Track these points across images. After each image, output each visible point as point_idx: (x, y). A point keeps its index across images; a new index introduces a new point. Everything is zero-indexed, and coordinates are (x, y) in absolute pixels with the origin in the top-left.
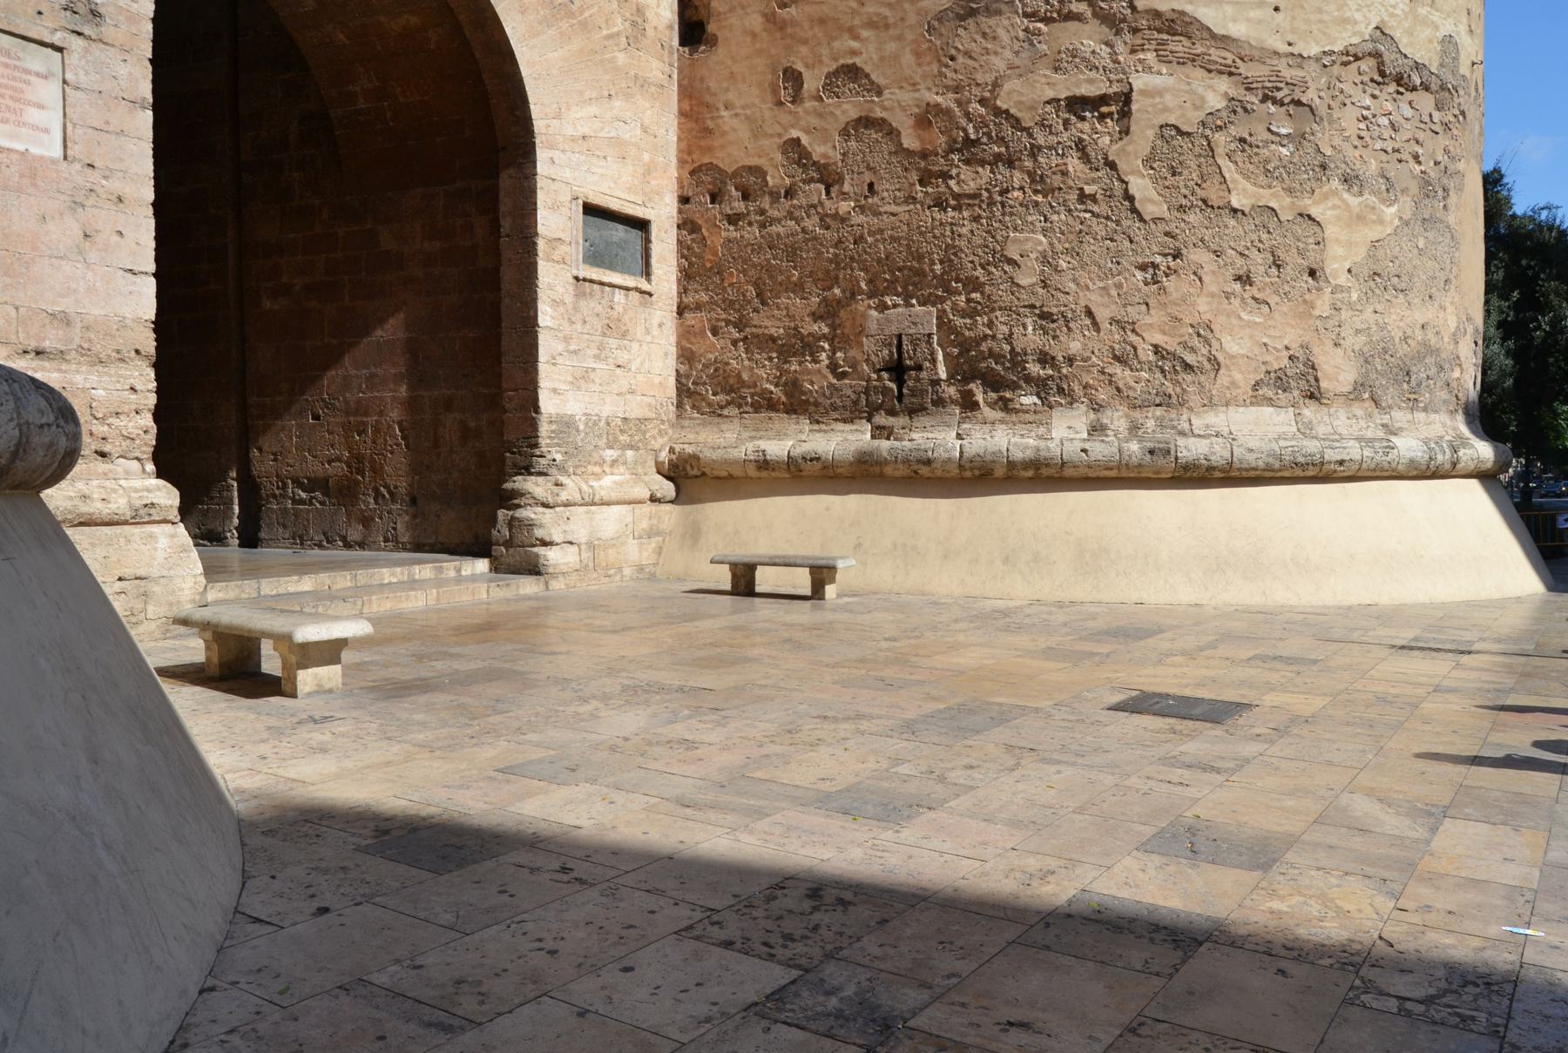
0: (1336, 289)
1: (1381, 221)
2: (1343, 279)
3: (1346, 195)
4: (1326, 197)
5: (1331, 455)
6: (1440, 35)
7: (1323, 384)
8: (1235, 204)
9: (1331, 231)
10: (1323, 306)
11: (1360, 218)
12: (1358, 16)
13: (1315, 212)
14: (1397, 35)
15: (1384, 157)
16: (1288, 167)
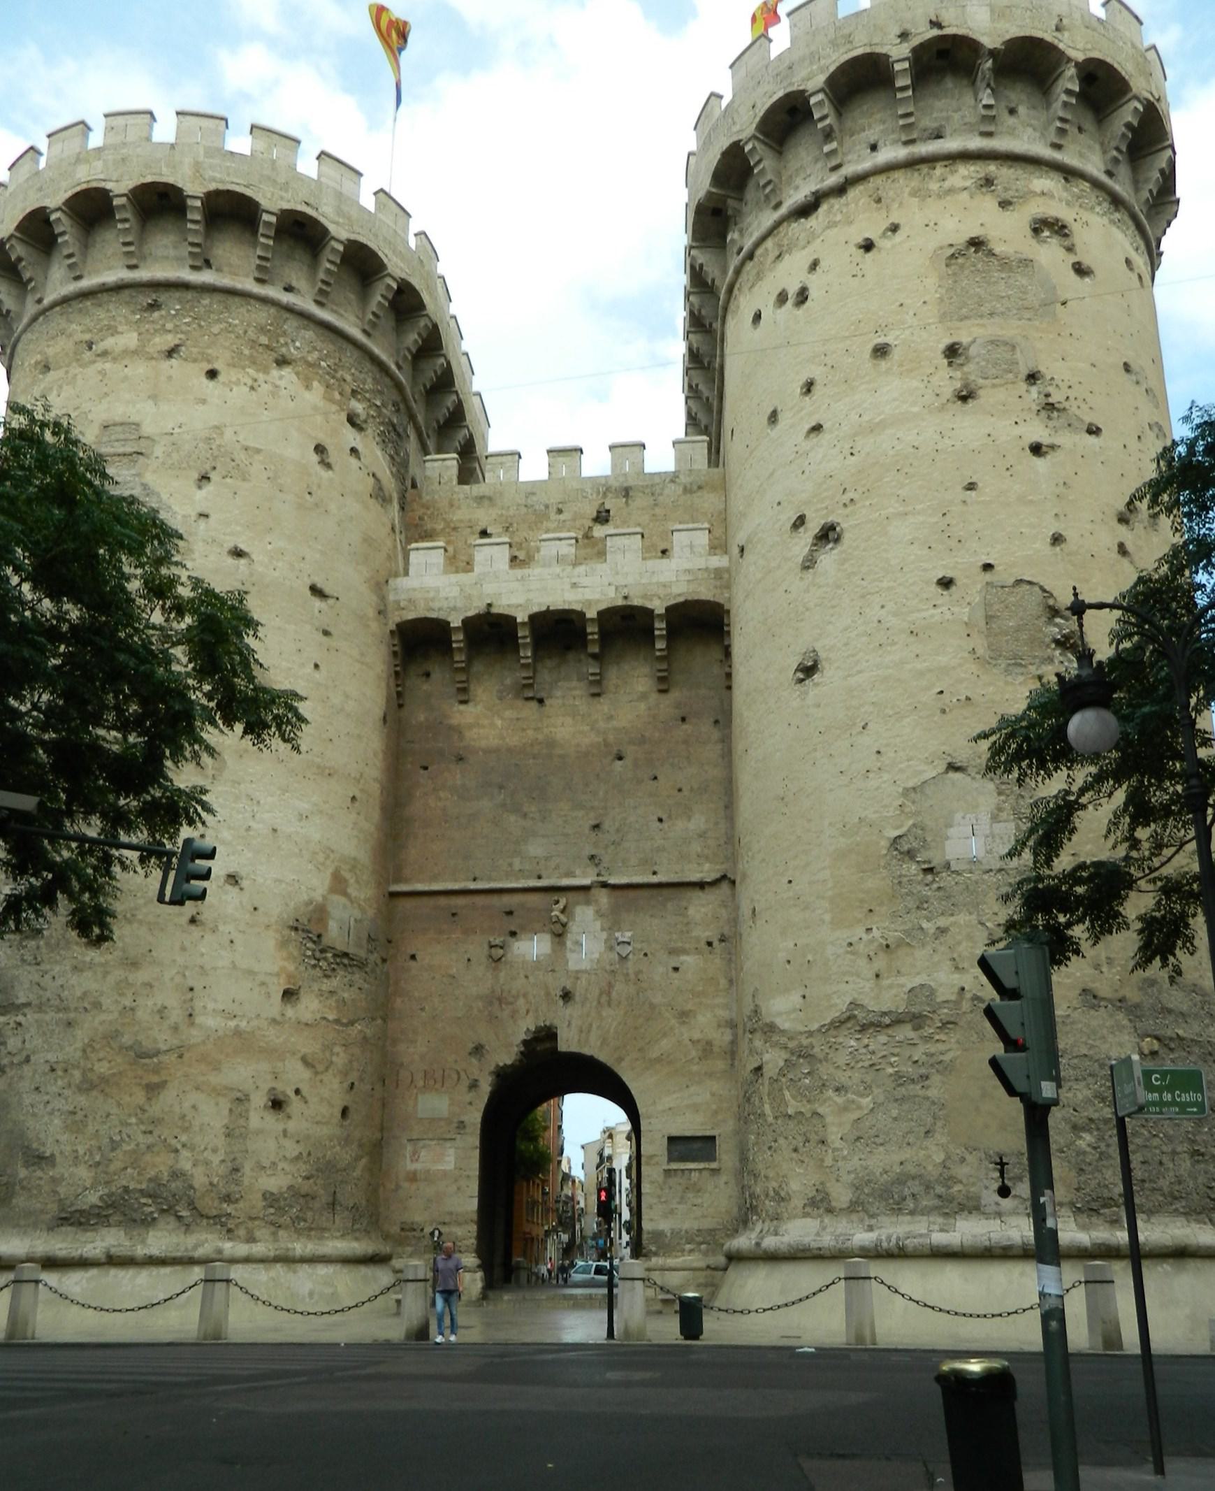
0: (834, 1150)
1: (860, 1107)
2: (838, 1144)
3: (836, 1099)
4: (825, 1101)
5: (814, 1245)
6: (906, 989)
7: (834, 1204)
8: (790, 1111)
9: (829, 1119)
10: (829, 1161)
11: (845, 1109)
12: (838, 1001)
13: (820, 1110)
14: (865, 1002)
15: (863, 1070)
16: (807, 1088)
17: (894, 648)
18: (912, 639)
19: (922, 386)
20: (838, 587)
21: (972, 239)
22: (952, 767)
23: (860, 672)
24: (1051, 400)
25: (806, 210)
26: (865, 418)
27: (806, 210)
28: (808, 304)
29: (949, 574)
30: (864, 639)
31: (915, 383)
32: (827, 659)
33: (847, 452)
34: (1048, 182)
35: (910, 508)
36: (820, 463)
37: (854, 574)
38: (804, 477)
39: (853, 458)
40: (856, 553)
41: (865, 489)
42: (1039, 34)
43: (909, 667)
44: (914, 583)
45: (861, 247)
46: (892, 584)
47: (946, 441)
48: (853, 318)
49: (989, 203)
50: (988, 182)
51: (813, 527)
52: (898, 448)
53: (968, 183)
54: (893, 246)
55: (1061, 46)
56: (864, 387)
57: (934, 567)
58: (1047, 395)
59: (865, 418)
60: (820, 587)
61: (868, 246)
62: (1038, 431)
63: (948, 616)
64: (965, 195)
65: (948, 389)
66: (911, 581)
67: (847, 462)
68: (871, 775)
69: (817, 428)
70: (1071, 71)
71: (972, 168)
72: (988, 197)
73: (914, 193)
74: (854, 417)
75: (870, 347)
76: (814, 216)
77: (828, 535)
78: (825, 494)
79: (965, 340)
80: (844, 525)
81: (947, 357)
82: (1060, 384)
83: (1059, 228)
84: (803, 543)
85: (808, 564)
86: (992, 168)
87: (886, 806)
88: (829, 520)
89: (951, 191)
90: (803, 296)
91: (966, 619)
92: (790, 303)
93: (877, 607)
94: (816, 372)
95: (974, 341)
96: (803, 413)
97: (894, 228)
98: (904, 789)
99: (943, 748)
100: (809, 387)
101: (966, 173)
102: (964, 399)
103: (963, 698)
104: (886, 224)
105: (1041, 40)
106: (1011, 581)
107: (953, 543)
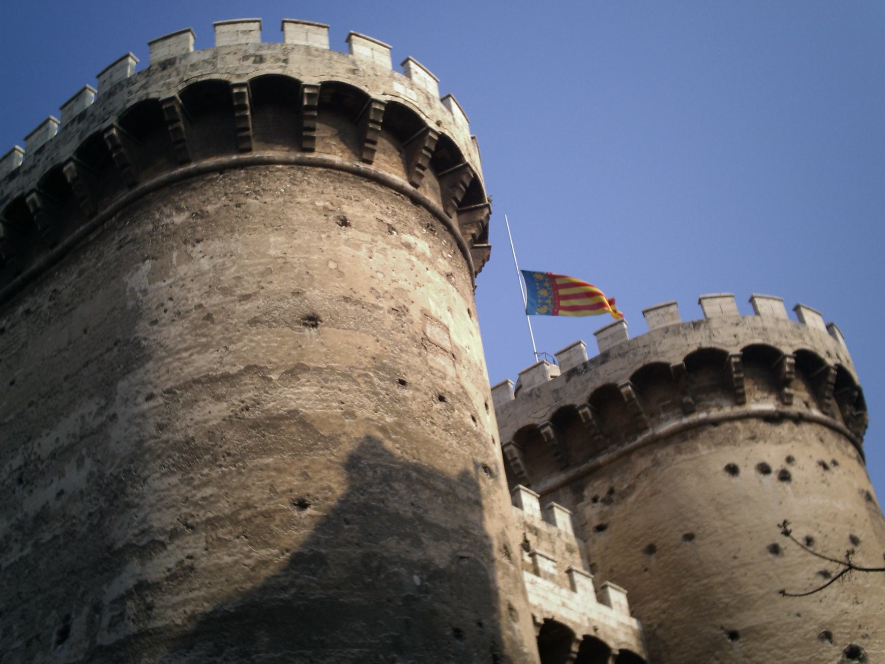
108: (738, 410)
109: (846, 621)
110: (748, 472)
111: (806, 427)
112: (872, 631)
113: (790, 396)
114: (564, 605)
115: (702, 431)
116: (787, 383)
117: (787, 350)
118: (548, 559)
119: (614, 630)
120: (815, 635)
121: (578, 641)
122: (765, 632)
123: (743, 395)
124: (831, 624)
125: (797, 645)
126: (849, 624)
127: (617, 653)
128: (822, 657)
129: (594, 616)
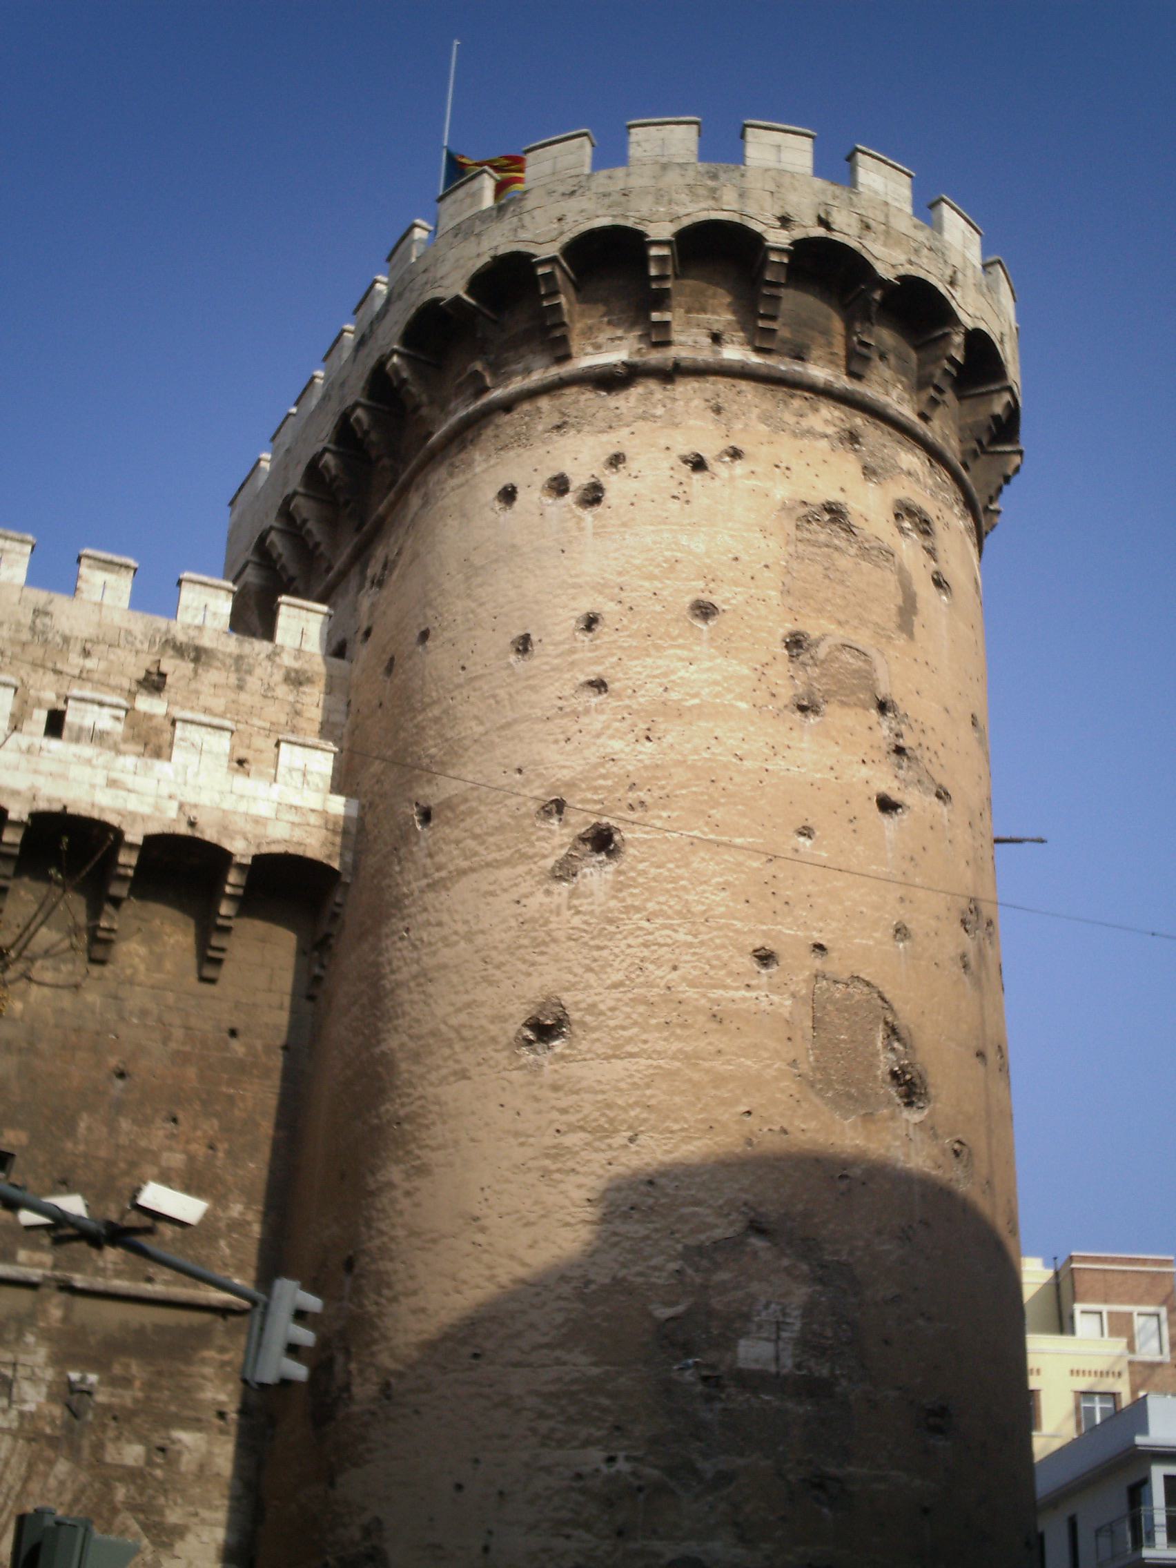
17: (687, 1033)
18: (714, 1026)
19: (754, 676)
20: (611, 921)
21: (829, 503)
22: (757, 1228)
23: (631, 1055)
24: (901, 742)
25: (611, 381)
26: (674, 696)
27: (611, 381)
28: (598, 509)
29: (771, 946)
30: (642, 1009)
31: (746, 671)
32: (583, 1024)
33: (642, 734)
34: (915, 460)
35: (725, 839)
36: (598, 736)
37: (638, 910)
38: (569, 747)
39: (648, 744)
40: (641, 880)
41: (662, 793)
42: (933, 280)
43: (707, 1065)
44: (723, 946)
45: (686, 461)
46: (690, 938)
47: (778, 759)
48: (668, 554)
49: (849, 464)
50: (853, 438)
51: (579, 822)
52: (713, 750)
53: (830, 430)
54: (732, 478)
55: (953, 304)
56: (672, 651)
57: (751, 931)
58: (899, 735)
59: (674, 696)
60: (578, 912)
61: (698, 464)
62: (887, 784)
63: (764, 1004)
64: (824, 444)
65: (786, 694)
66: (718, 941)
67: (639, 747)
68: (636, 1215)
69: (599, 685)
70: (958, 339)
71: (837, 413)
72: (852, 456)
73: (765, 418)
74: (654, 688)
75: (688, 600)
76: (623, 395)
77: (602, 841)
78: (601, 782)
79: (814, 634)
80: (627, 835)
81: (787, 646)
82: (914, 725)
83: (925, 527)
84: (556, 841)
85: (565, 871)
86: (859, 420)
87: (655, 1268)
88: (605, 820)
89: (810, 432)
90: (593, 496)
91: (787, 1015)
92: (569, 498)
93: (666, 968)
94: (607, 608)
95: (823, 638)
96: (576, 657)
97: (736, 454)
98: (686, 1247)
99: (745, 1196)
100: (591, 622)
101: (829, 417)
102: (802, 709)
103: (776, 1128)
104: (723, 445)
105: (934, 289)
106: (845, 976)
107: (779, 906)
108: (555, 372)
109: (604, 777)
110: (531, 496)
111: (685, 388)
112: (657, 793)
113: (666, 325)
114: (112, 783)
115: (485, 427)
116: (661, 300)
117: (661, 231)
118: (101, 704)
119: (257, 821)
120: (533, 806)
121: (132, 846)
122: (462, 808)
123: (564, 341)
124: (571, 785)
125: (501, 829)
126: (610, 782)
127: (248, 861)
128: (531, 851)
129: (205, 799)
